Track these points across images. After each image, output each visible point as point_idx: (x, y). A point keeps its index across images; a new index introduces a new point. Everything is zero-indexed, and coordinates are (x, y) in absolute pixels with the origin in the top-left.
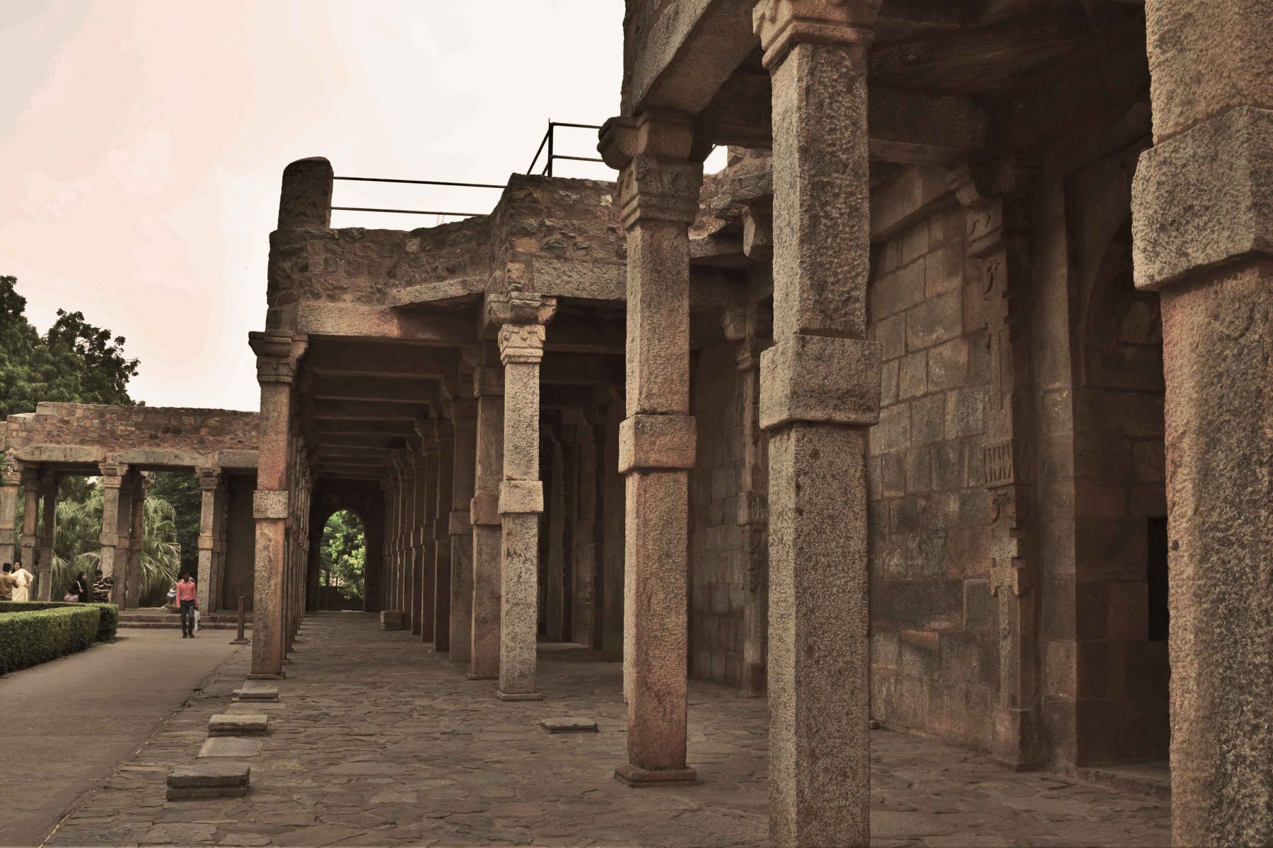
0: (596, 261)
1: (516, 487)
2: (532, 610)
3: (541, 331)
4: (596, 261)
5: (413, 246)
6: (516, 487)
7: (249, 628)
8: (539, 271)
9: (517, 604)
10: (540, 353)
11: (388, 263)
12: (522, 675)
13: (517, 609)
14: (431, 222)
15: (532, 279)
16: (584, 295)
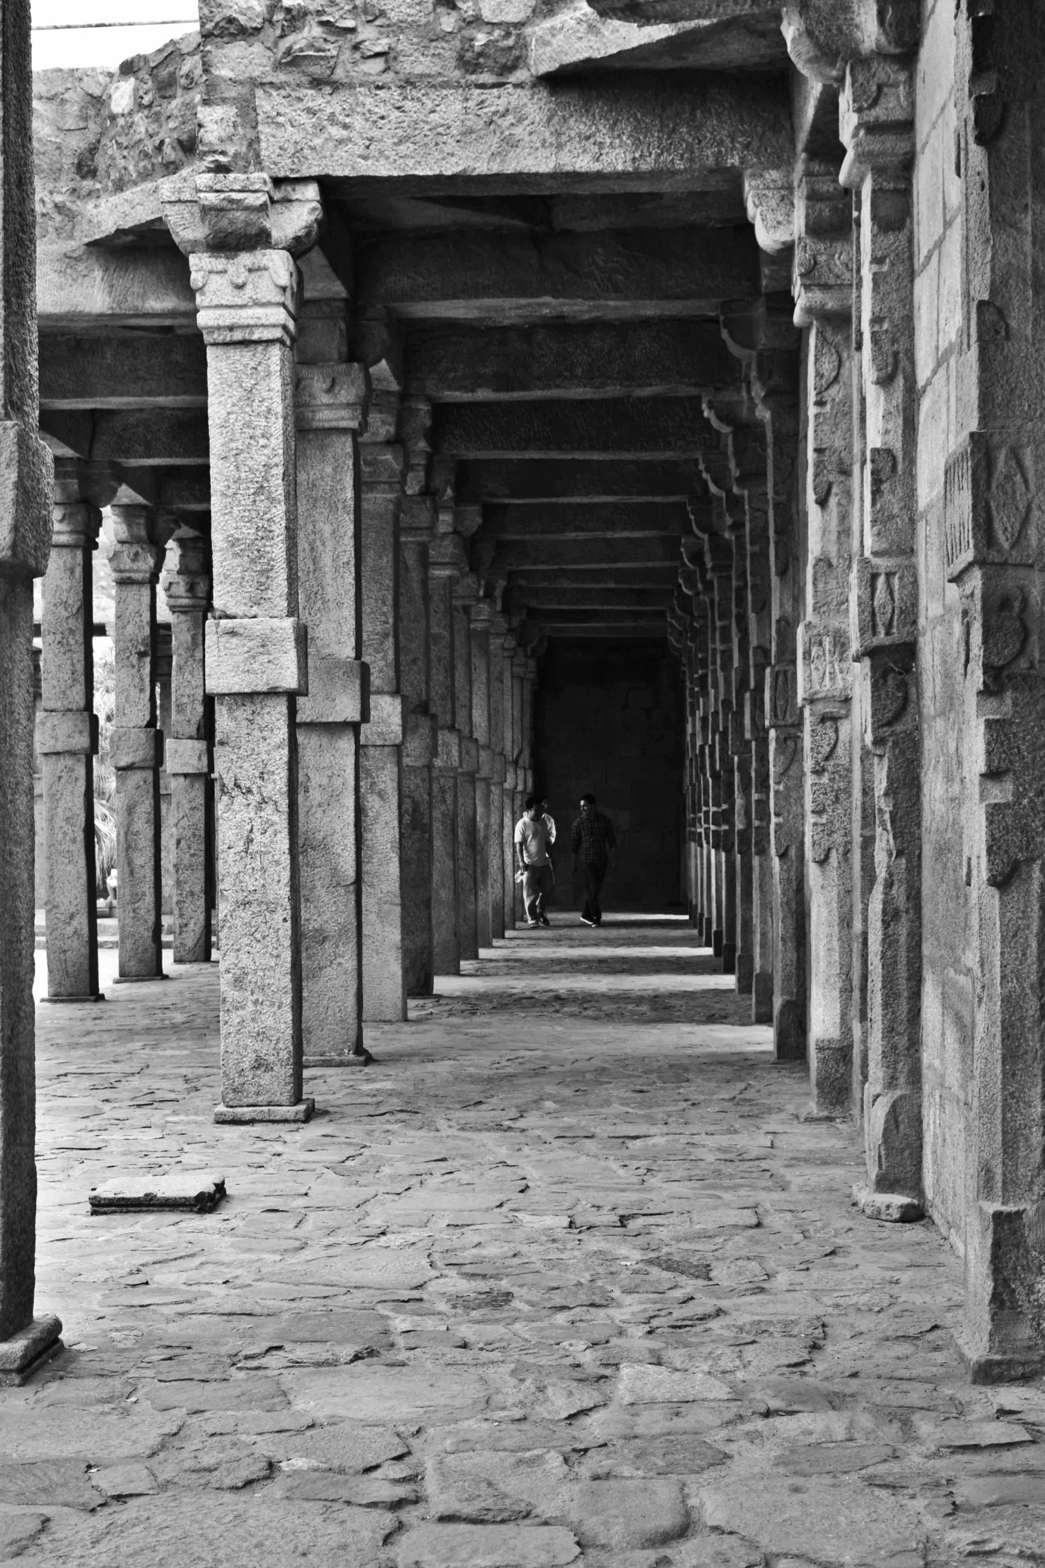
0: (409, 82)
1: (233, 633)
2: (279, 916)
3: (278, 266)
4: (409, 82)
5: (122, 97)
6: (233, 633)
7: (169, 945)
8: (271, 121)
9: (246, 904)
10: (280, 316)
11: (76, 143)
12: (260, 1064)
13: (246, 915)
14: (148, 43)
15: (254, 143)
16: (382, 169)
